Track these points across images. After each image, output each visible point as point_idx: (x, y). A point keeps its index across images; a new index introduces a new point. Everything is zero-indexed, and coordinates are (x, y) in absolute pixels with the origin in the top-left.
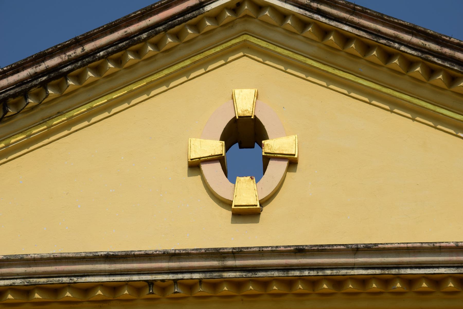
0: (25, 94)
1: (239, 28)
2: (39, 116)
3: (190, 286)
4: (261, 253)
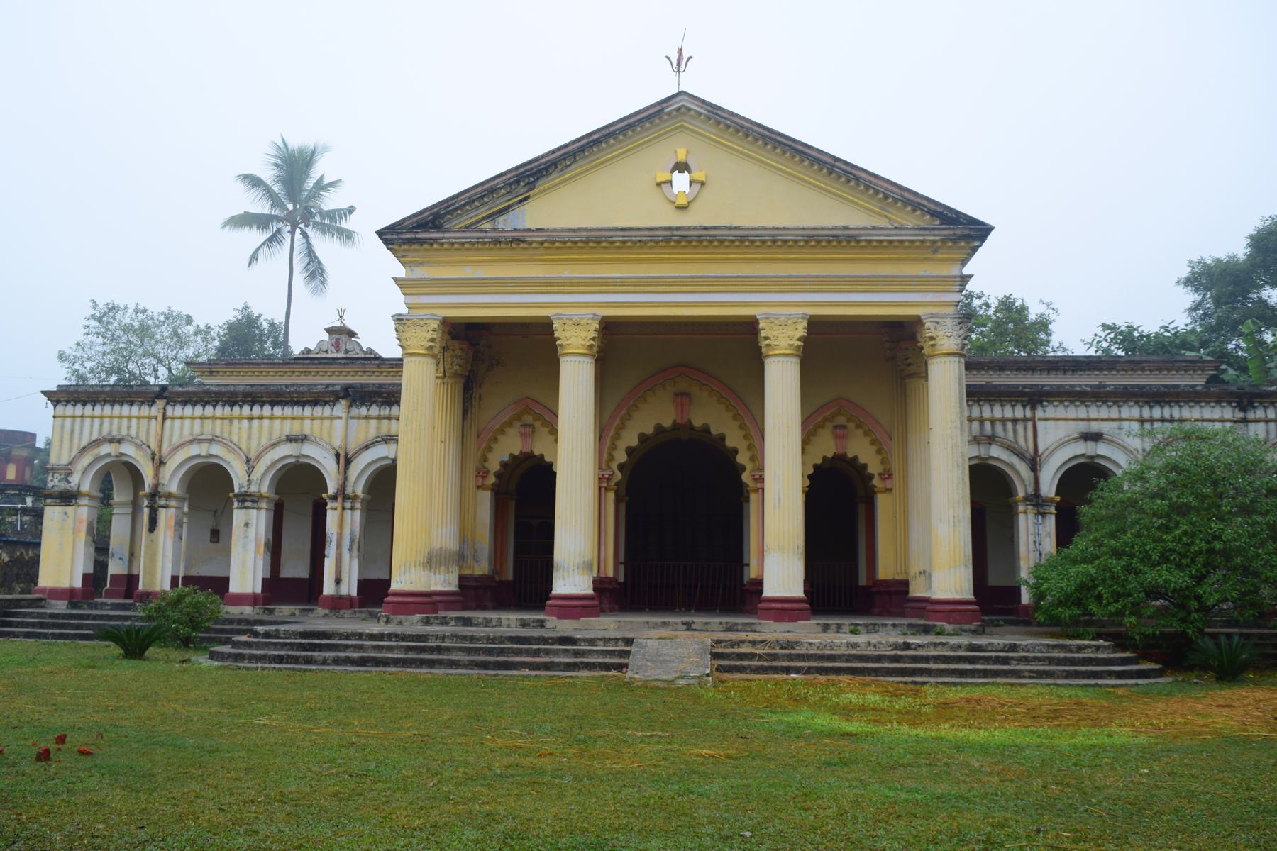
3: (657, 242)
4: (689, 228)
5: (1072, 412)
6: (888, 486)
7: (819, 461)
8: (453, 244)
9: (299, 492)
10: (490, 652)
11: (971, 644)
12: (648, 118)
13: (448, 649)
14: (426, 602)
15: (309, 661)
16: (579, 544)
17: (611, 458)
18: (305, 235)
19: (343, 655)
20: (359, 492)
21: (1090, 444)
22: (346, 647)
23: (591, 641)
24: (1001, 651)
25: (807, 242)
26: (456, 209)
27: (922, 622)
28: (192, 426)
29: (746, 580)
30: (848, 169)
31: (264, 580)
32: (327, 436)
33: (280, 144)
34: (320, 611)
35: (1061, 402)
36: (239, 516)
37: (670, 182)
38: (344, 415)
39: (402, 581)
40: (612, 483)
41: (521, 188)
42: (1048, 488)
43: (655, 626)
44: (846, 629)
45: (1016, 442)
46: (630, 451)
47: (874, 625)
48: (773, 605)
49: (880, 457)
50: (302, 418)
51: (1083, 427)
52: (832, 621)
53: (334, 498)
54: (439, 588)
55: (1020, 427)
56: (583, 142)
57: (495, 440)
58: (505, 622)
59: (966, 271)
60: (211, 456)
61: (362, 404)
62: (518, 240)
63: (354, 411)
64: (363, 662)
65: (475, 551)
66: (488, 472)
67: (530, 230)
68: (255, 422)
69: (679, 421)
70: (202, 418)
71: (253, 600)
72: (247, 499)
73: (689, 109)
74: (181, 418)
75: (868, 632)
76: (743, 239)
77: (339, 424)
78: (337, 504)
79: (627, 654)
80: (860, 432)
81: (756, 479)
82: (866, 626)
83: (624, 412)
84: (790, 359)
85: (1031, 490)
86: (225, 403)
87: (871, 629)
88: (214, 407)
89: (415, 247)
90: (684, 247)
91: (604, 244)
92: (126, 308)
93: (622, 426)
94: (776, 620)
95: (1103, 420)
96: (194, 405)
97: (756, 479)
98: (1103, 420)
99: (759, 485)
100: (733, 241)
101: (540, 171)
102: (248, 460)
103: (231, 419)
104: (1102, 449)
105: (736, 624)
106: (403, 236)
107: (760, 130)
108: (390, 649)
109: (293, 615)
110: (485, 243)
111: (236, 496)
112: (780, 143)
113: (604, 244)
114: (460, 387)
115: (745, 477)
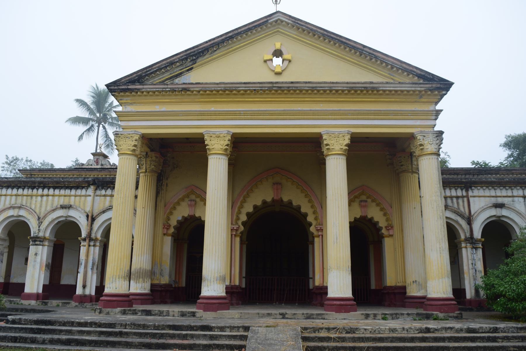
0: (223, 42)
1: (277, 27)
2: (226, 48)
3: (264, 91)
4: (282, 83)
5: (487, 193)
6: (391, 233)
7: (353, 220)
8: (149, 92)
9: (65, 238)
10: (154, 336)
11: (468, 328)
12: (259, 25)
13: (127, 334)
14: (126, 301)
15: (33, 341)
16: (218, 265)
17: (238, 219)
18: (104, 128)
19: (56, 337)
20: (99, 236)
21: (498, 210)
22: (61, 331)
23: (222, 329)
24: (488, 332)
25: (349, 91)
26: (152, 73)
27: (425, 312)
28: (11, 200)
29: (311, 287)
30: (371, 52)
31: (44, 286)
32: (81, 205)
33: (95, 87)
34: (73, 304)
35: (482, 187)
36: (32, 249)
37: (272, 60)
38: (92, 194)
39: (114, 286)
40: (239, 232)
41: (188, 63)
42: (478, 234)
43: (263, 316)
44: (379, 317)
45: (459, 208)
46: (248, 214)
47: (396, 314)
48: (335, 302)
49: (385, 218)
50: (70, 196)
51: (494, 200)
52: (371, 311)
53: (84, 240)
54: (138, 291)
55: (460, 201)
56: (223, 37)
57: (174, 208)
58: (171, 313)
59: (438, 107)
60: (20, 216)
61: (102, 188)
62: (185, 90)
63: (98, 192)
64: (68, 342)
65: (162, 270)
66: (170, 226)
67: (192, 84)
68: (45, 198)
69: (275, 198)
70: (16, 195)
71: (37, 297)
72: (38, 240)
73: (282, 21)
74: (5, 195)
75: (393, 319)
76: (313, 89)
77: (89, 199)
78: (86, 243)
79: (245, 338)
80: (374, 204)
81: (318, 230)
82: (392, 315)
83: (245, 193)
84: (341, 157)
85: (468, 235)
86: (29, 188)
87: (395, 317)
88: (23, 189)
89: (127, 94)
90: (280, 94)
91: (234, 92)
92: (22, 159)
93: (244, 201)
94: (336, 312)
95: (504, 197)
96: (13, 189)
97: (318, 230)
98: (504, 197)
99: (320, 233)
100: (307, 91)
101: (199, 53)
102: (39, 218)
103: (32, 196)
104: (504, 212)
105: (313, 314)
106: (121, 87)
107: (322, 31)
108: (89, 333)
109: (58, 306)
110: (166, 92)
111: (31, 238)
112: (332, 38)
113: (234, 92)
114: (156, 178)
115: (312, 229)
